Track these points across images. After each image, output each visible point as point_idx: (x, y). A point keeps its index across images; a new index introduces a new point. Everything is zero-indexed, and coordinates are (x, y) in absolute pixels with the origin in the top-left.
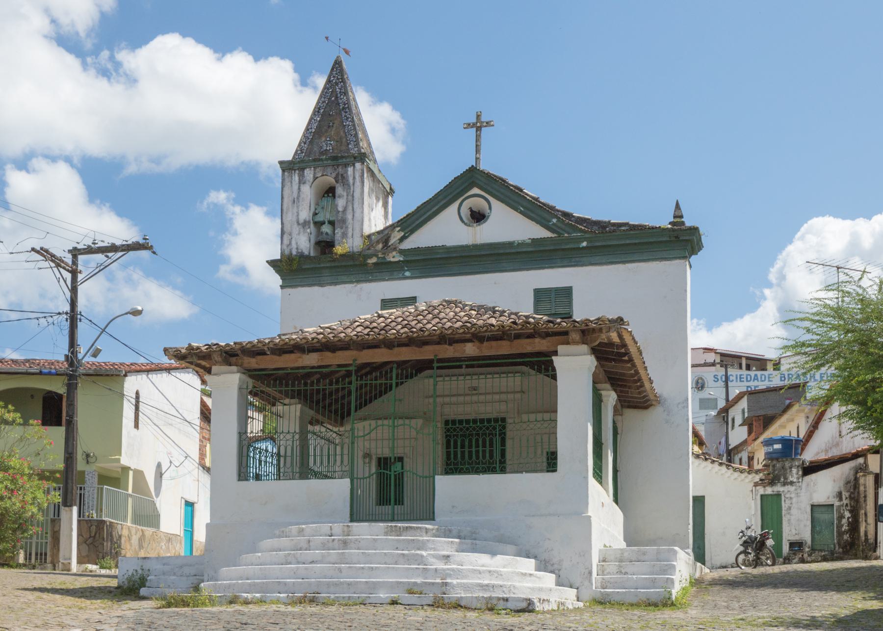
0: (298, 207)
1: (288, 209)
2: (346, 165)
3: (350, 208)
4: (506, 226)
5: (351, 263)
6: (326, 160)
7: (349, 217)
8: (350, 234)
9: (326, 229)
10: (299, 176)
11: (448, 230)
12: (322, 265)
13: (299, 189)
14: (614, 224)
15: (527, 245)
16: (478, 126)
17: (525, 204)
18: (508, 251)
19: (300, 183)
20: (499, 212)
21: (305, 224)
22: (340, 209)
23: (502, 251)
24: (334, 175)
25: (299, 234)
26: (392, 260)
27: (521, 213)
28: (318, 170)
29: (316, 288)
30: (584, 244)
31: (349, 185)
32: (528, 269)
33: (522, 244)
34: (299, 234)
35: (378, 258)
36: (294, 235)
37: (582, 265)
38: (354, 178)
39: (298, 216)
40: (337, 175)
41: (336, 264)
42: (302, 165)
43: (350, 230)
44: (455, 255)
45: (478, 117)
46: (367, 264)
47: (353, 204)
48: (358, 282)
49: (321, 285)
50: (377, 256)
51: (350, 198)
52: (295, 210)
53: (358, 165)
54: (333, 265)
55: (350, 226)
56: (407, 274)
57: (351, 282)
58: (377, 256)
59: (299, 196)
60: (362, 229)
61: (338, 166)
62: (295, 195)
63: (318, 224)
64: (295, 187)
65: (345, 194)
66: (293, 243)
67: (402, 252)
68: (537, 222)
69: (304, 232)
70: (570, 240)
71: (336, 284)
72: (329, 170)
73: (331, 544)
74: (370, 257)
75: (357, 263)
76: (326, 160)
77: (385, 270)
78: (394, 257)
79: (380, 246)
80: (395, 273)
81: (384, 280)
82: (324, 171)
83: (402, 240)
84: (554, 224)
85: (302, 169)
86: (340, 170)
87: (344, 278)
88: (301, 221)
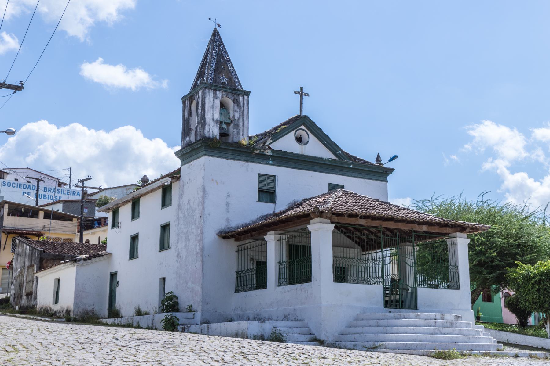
0: (213, 111)
1: (208, 110)
2: (239, 95)
3: (241, 119)
4: (314, 148)
5: (246, 150)
6: (229, 89)
7: (241, 124)
8: (241, 133)
9: (225, 126)
10: (214, 93)
11: (287, 143)
12: (231, 148)
13: (214, 101)
14: (359, 159)
15: (329, 161)
16: (301, 93)
17: (328, 141)
18: (320, 162)
19: (214, 97)
20: (313, 139)
21: (217, 121)
22: (236, 118)
23: (317, 161)
24: (232, 98)
25: (214, 126)
26: (267, 154)
27: (324, 144)
28: (224, 93)
29: (224, 160)
30: (351, 166)
31: (240, 106)
32: (326, 173)
33: (326, 160)
34: (214, 126)
35: (260, 151)
36: (211, 126)
37: (348, 176)
38: (244, 103)
39: (213, 115)
40: (235, 99)
41: (238, 149)
42: (216, 88)
43: (241, 131)
44: (296, 158)
45: (302, 89)
46: (251, 153)
47: (243, 118)
48: (247, 161)
49: (227, 159)
50: (260, 150)
51: (241, 114)
52: (211, 112)
53: (246, 97)
54: (236, 149)
55: (241, 129)
56: (271, 162)
57: (243, 161)
58: (260, 150)
59: (213, 105)
60: (248, 133)
61: (235, 94)
62: (212, 103)
63: (221, 122)
64: (212, 99)
65: (239, 111)
66: (211, 131)
67: (273, 151)
68: (331, 150)
69: (217, 126)
70: (346, 163)
71: (235, 160)
72: (230, 95)
73: (446, 324)
74: (257, 150)
75: (249, 151)
76: (229, 89)
77: (262, 158)
78: (268, 153)
79: (262, 145)
80: (265, 161)
81: (260, 163)
82: (227, 94)
83: (270, 144)
84: (339, 154)
85: (215, 90)
86: (236, 96)
87: (239, 157)
88: (215, 119)
